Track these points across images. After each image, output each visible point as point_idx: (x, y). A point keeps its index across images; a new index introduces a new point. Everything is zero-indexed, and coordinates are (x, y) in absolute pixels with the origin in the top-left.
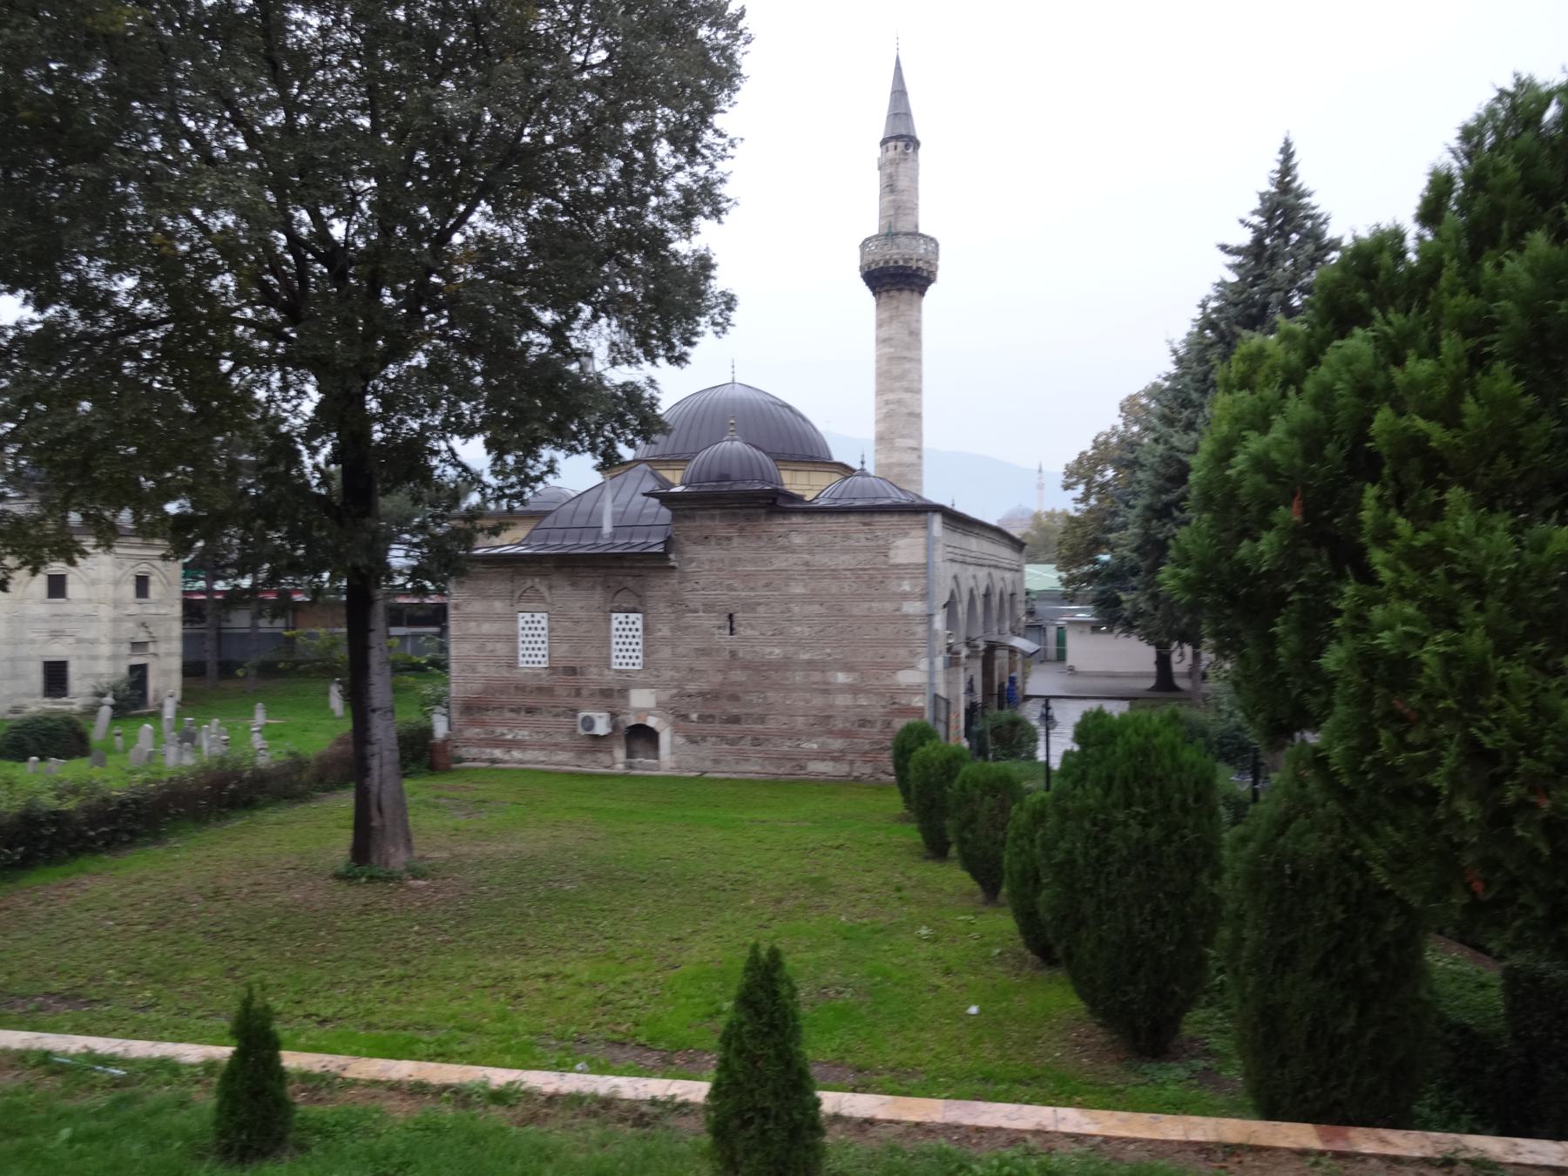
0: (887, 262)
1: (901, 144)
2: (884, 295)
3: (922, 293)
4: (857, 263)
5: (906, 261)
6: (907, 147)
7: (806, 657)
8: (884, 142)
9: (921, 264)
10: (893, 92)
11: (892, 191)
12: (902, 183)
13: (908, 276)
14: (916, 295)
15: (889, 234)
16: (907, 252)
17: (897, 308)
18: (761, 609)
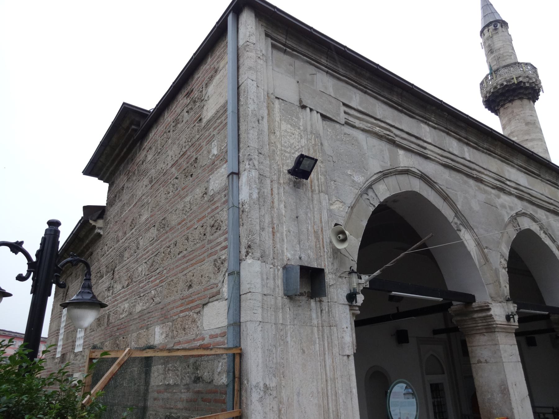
0: (495, 87)
1: (492, 27)
2: (502, 110)
3: (534, 102)
4: (481, 99)
5: (507, 81)
6: (495, 26)
7: (139, 308)
8: (482, 32)
9: (521, 79)
10: (482, 8)
11: (492, 53)
12: (498, 43)
13: (514, 90)
14: (525, 101)
15: (493, 72)
16: (507, 76)
17: (513, 112)
18: (126, 255)
